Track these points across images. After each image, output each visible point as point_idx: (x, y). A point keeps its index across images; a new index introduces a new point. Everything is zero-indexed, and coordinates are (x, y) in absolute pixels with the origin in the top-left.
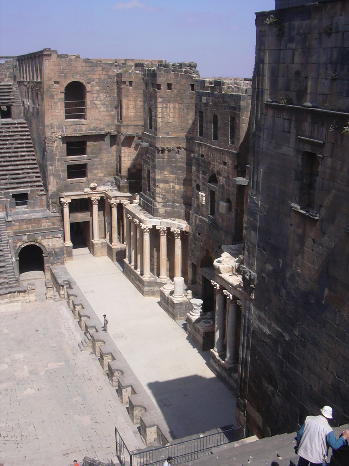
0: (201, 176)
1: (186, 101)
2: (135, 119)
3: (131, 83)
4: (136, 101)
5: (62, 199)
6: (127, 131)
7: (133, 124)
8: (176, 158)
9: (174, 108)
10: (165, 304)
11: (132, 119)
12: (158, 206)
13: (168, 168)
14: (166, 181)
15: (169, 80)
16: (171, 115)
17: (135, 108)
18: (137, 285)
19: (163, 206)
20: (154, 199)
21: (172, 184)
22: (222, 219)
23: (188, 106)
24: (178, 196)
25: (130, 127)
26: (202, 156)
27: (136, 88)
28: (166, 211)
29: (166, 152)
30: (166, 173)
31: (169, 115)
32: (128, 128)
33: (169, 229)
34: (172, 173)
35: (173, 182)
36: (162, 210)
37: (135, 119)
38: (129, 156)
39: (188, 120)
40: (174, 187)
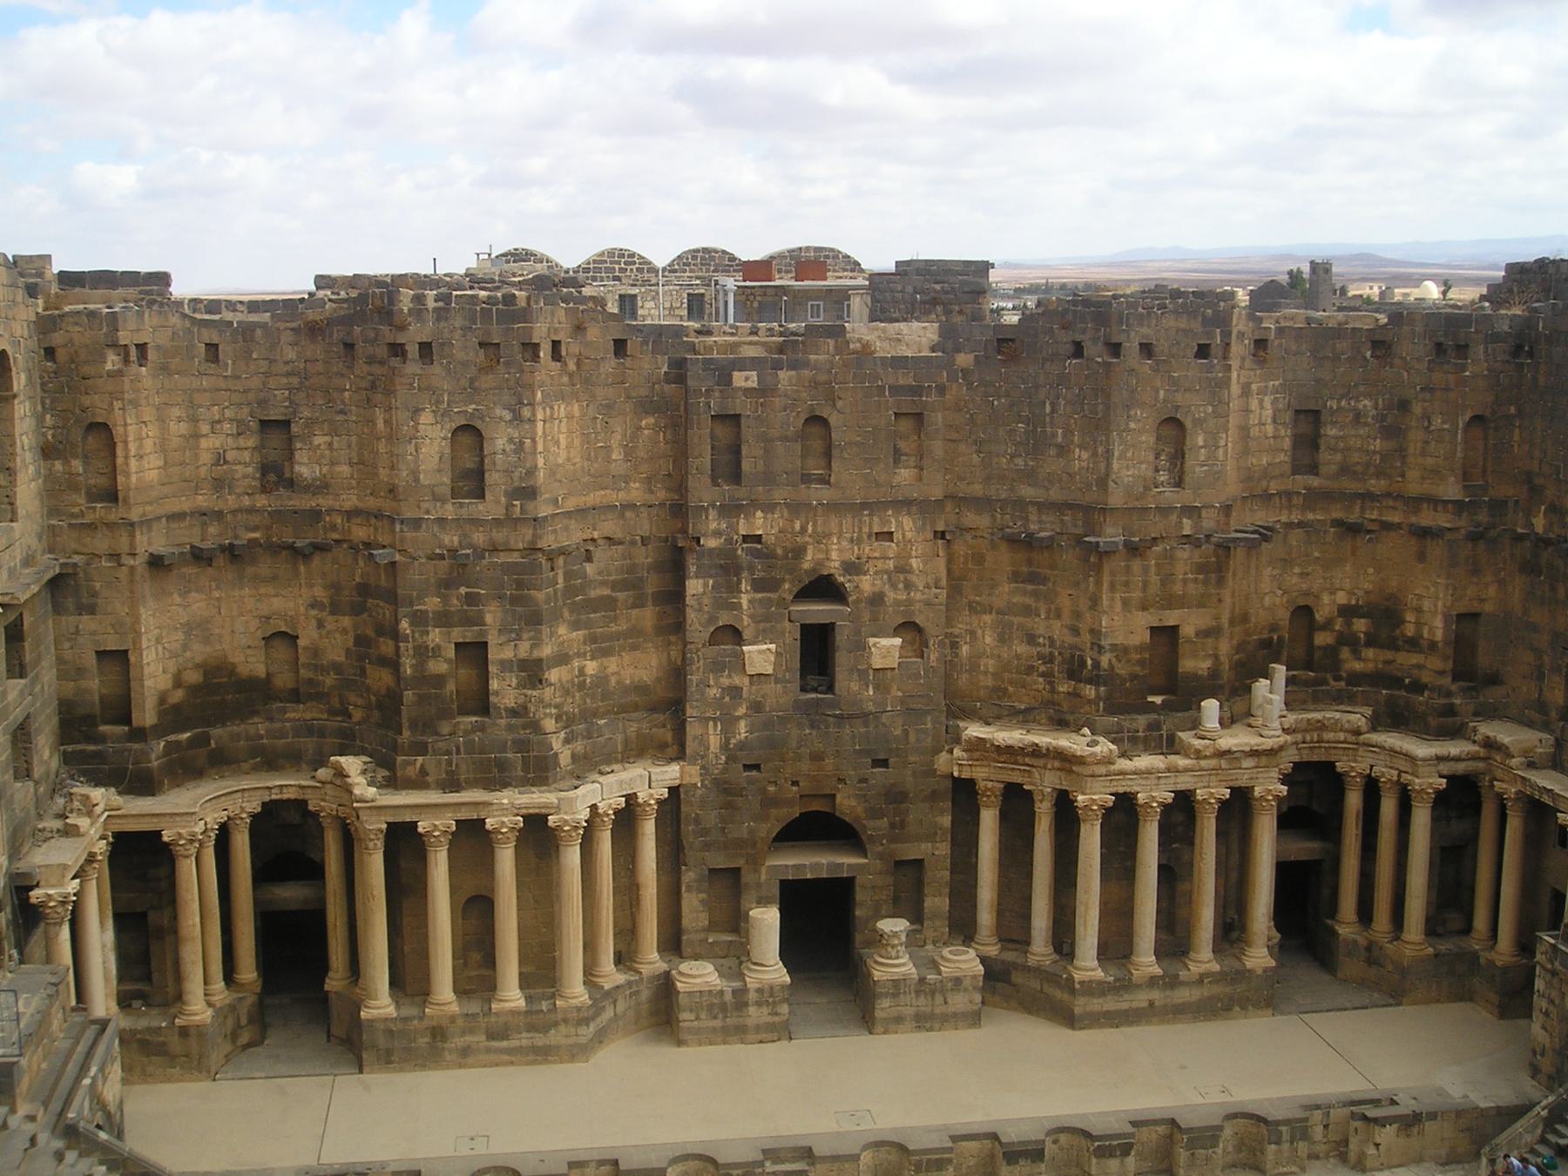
0: (744, 600)
1: (600, 392)
2: (166, 490)
3: (142, 348)
4: (162, 420)
5: (36, 895)
6: (150, 544)
7: (160, 511)
8: (584, 576)
9: (570, 417)
10: (718, 1023)
11: (154, 494)
12: (556, 743)
13: (566, 614)
14: (562, 659)
15: (556, 330)
16: (563, 443)
17: (163, 448)
18: (509, 1051)
19: (567, 741)
20: (535, 726)
21: (576, 664)
22: (876, 688)
23: (609, 407)
24: (593, 697)
25: (155, 526)
26: (746, 538)
27: (164, 369)
28: (573, 756)
29: (561, 561)
30: (562, 630)
31: (557, 443)
32: (150, 530)
33: (631, 798)
34: (576, 626)
35: (580, 655)
36: (565, 759)
37: (166, 490)
38: (158, 640)
39: (608, 449)
40: (582, 671)
